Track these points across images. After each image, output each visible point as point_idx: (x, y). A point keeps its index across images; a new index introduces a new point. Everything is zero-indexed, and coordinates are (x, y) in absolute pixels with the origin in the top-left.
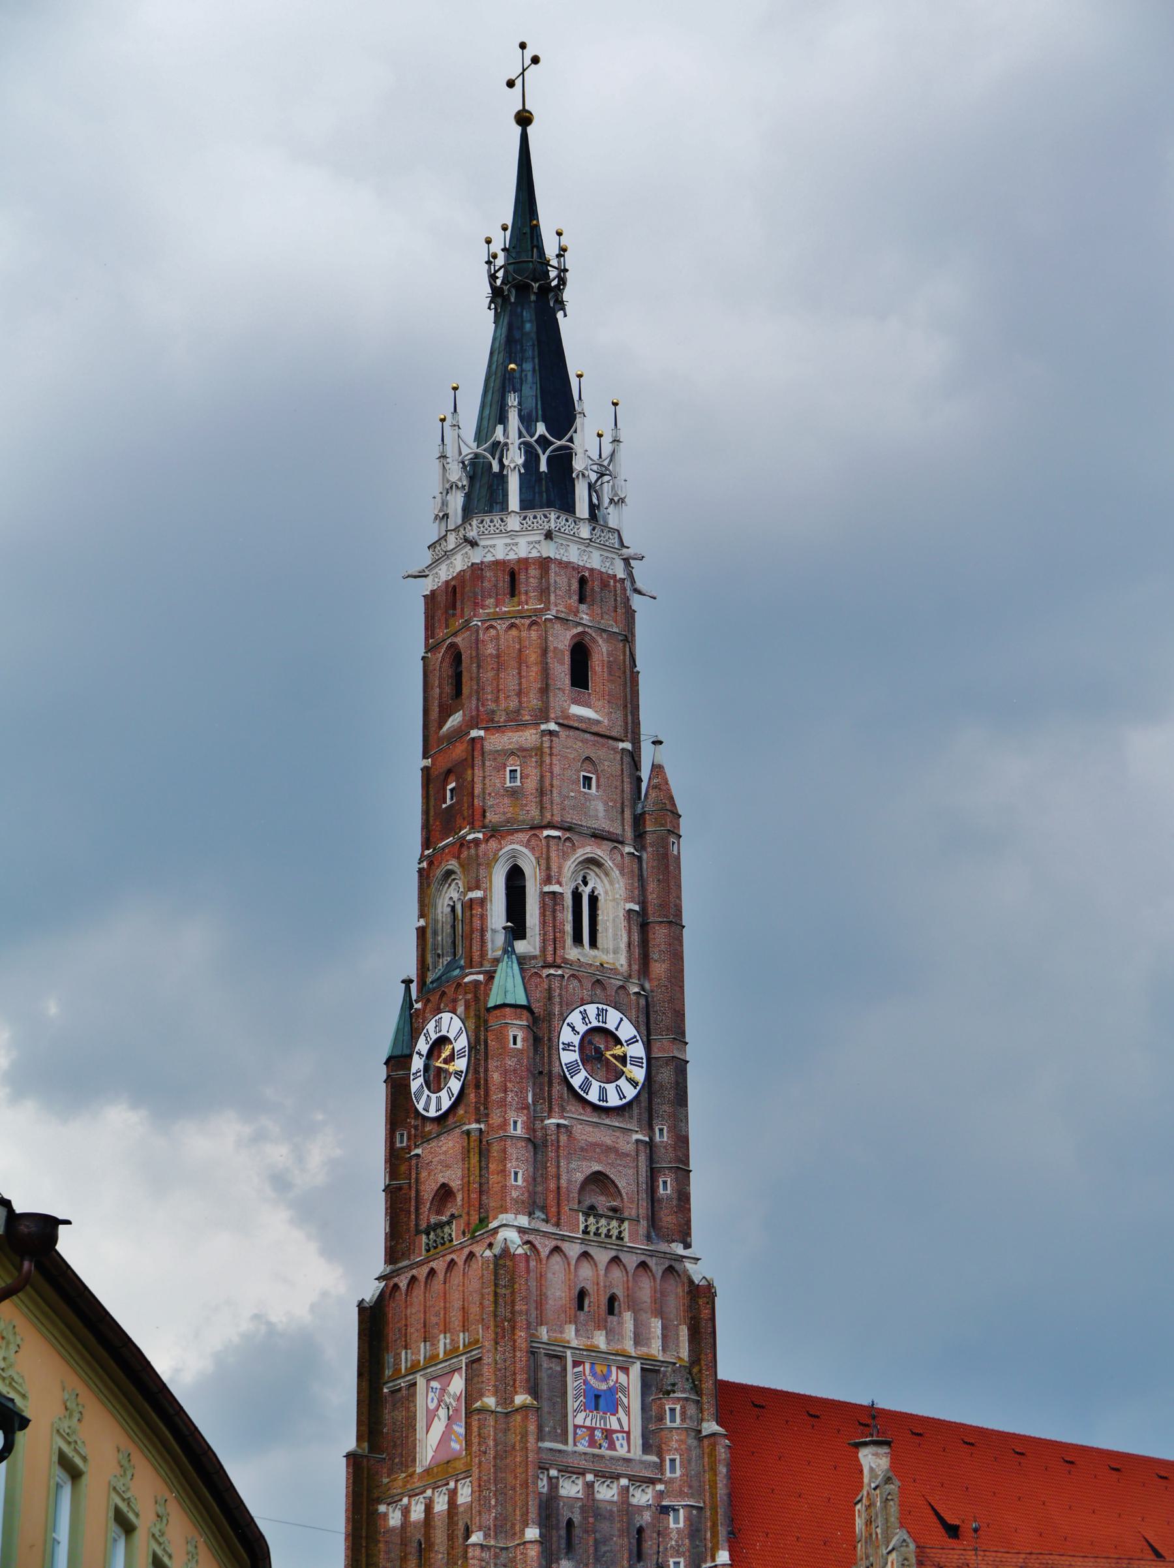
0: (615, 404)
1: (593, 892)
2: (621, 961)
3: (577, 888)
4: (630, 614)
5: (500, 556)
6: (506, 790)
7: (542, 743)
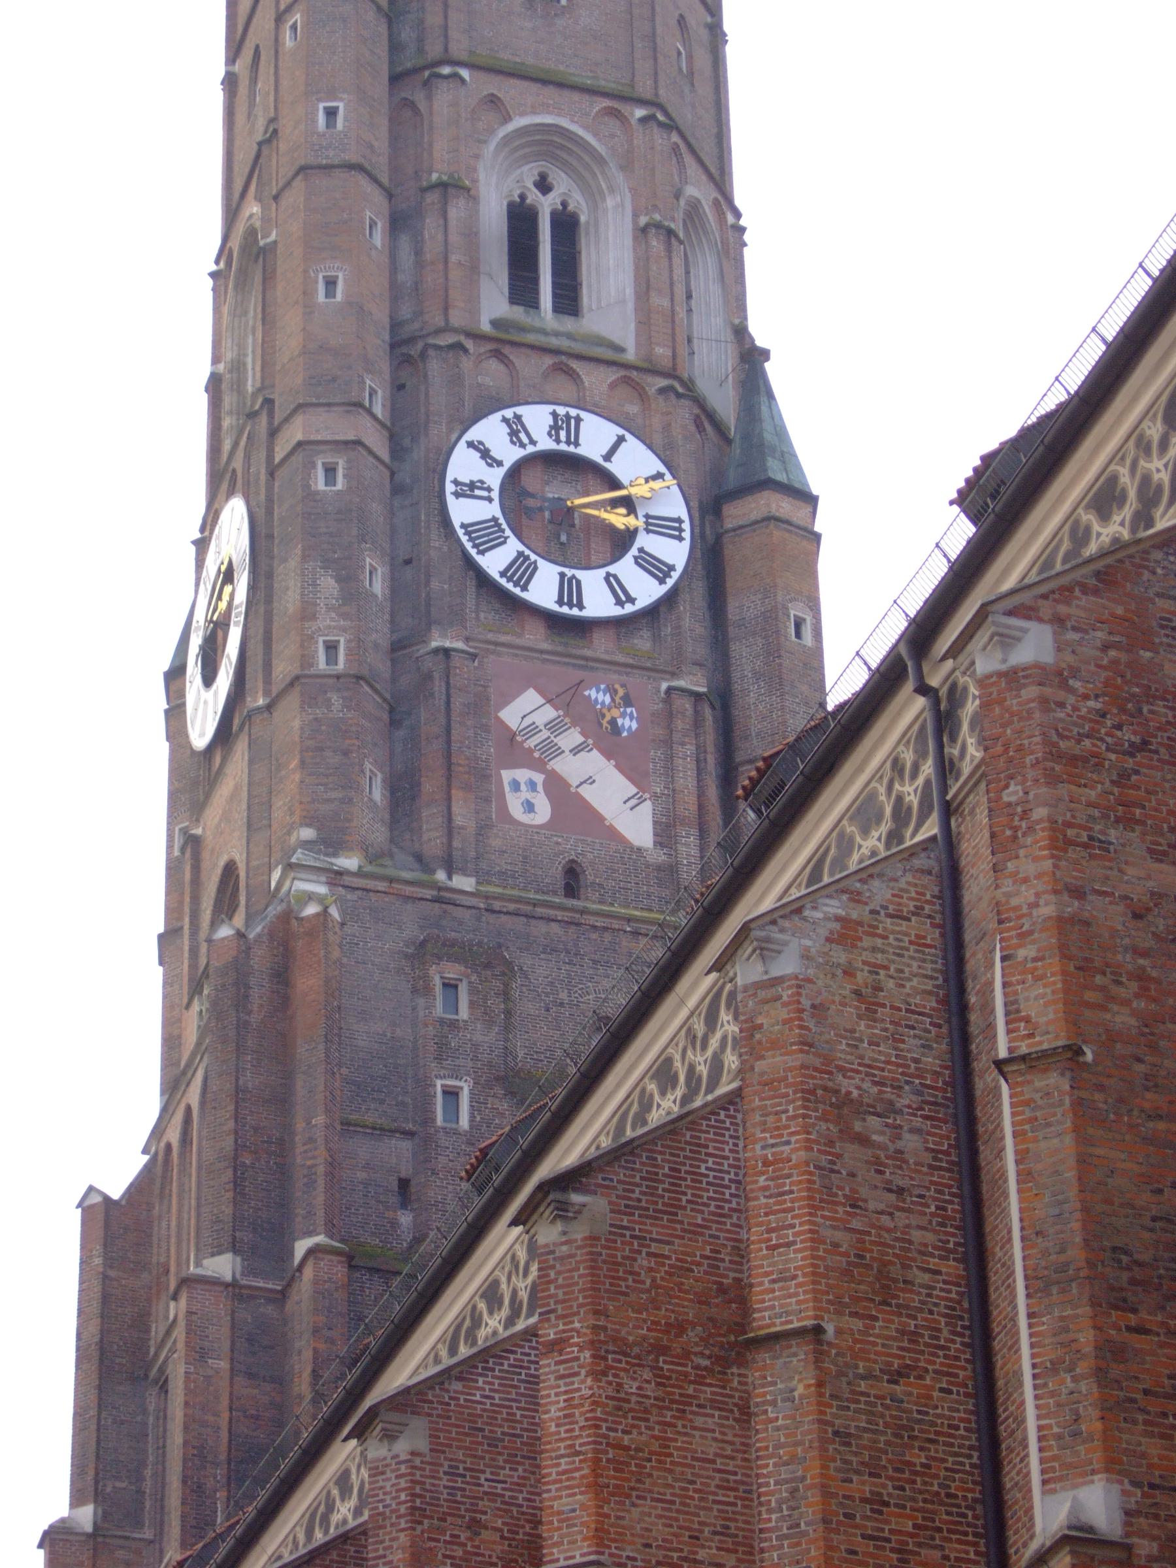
1: (564, 204)
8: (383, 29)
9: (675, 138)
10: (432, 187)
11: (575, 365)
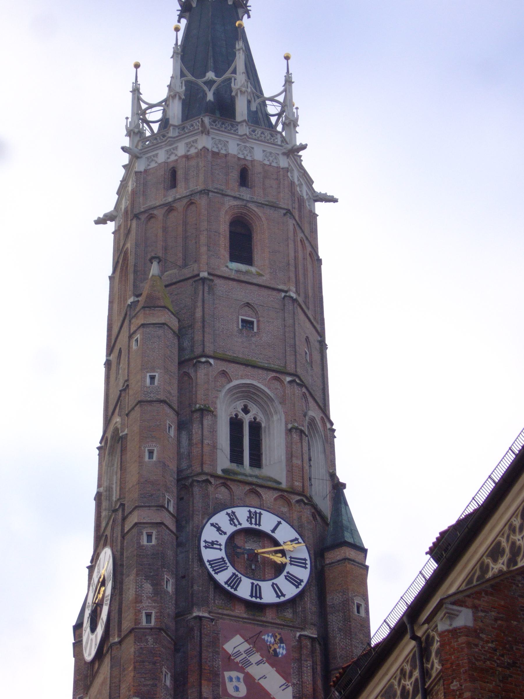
1: (255, 419)
8: (176, 341)
9: (304, 390)
10: (196, 411)
11: (259, 490)
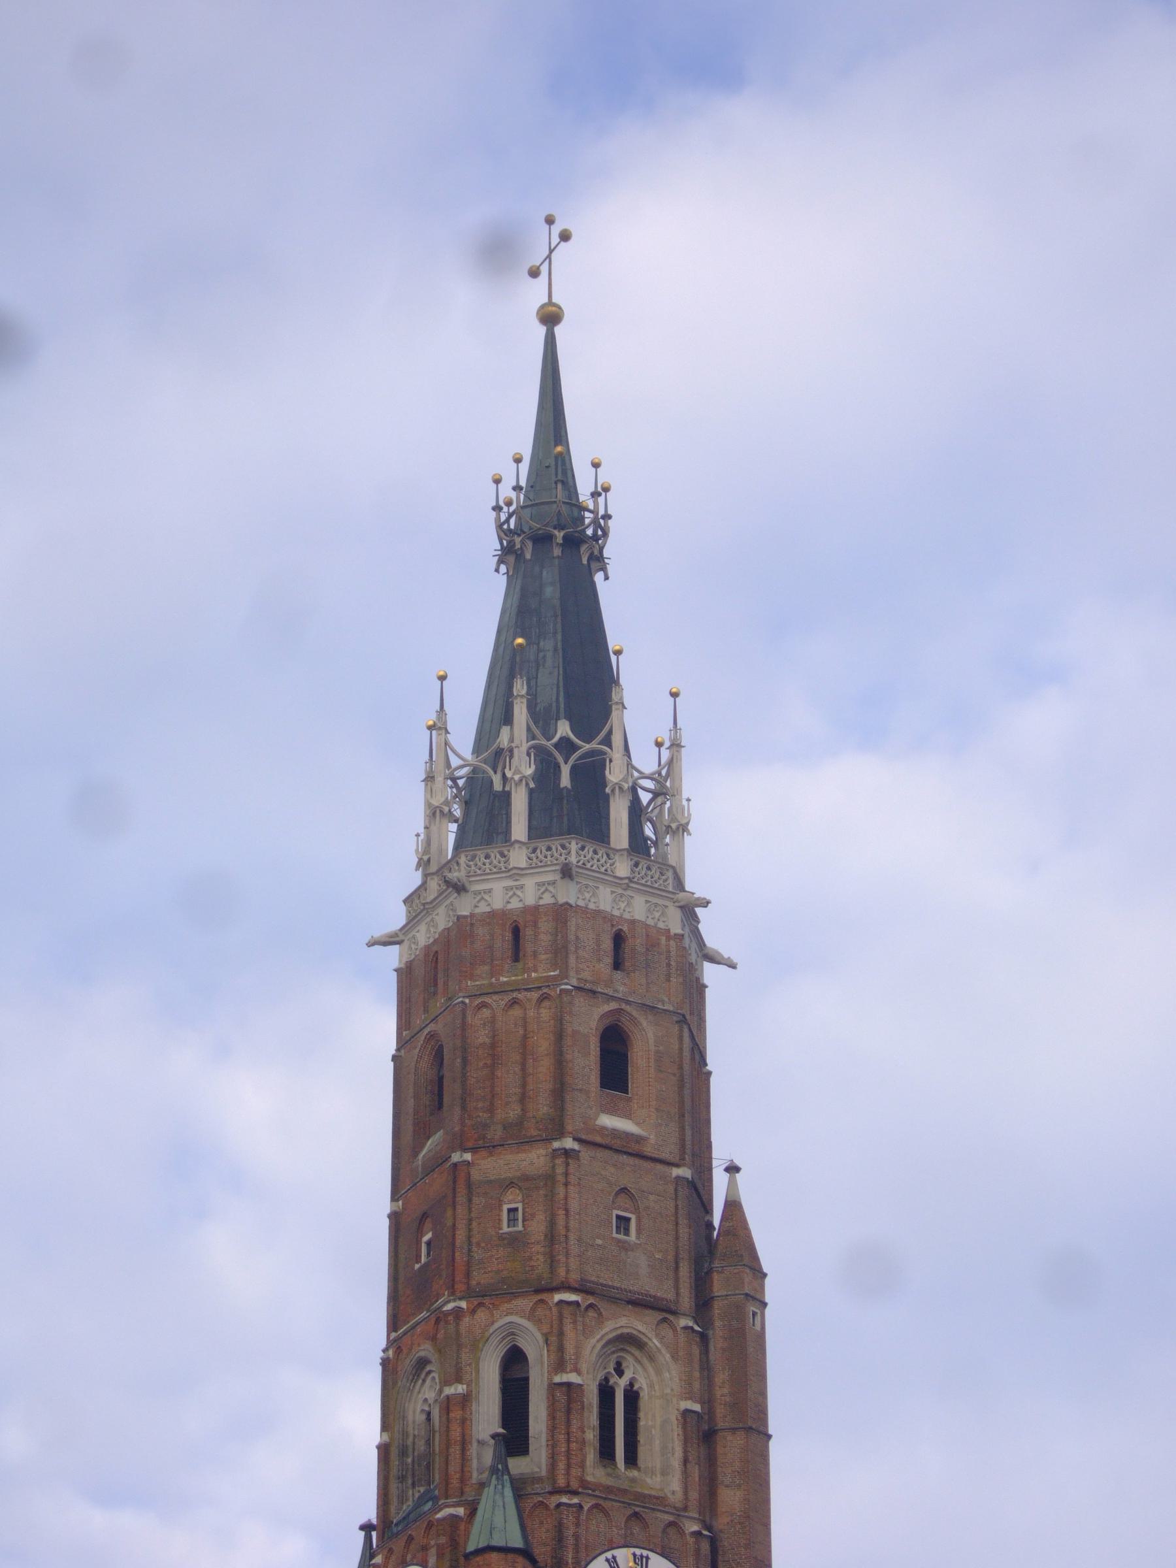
0: (675, 695)
1: (631, 1385)
2: (674, 1487)
3: (606, 1379)
4: (696, 991)
5: (498, 903)
6: (501, 1237)
7: (553, 1167)
